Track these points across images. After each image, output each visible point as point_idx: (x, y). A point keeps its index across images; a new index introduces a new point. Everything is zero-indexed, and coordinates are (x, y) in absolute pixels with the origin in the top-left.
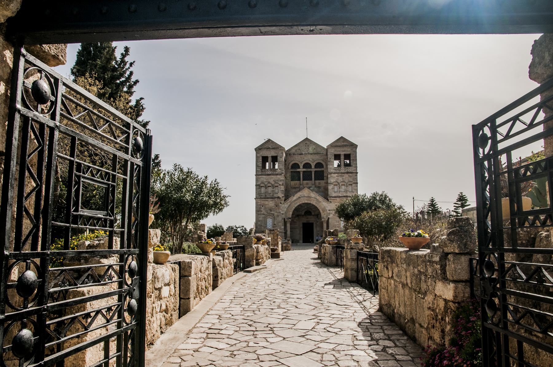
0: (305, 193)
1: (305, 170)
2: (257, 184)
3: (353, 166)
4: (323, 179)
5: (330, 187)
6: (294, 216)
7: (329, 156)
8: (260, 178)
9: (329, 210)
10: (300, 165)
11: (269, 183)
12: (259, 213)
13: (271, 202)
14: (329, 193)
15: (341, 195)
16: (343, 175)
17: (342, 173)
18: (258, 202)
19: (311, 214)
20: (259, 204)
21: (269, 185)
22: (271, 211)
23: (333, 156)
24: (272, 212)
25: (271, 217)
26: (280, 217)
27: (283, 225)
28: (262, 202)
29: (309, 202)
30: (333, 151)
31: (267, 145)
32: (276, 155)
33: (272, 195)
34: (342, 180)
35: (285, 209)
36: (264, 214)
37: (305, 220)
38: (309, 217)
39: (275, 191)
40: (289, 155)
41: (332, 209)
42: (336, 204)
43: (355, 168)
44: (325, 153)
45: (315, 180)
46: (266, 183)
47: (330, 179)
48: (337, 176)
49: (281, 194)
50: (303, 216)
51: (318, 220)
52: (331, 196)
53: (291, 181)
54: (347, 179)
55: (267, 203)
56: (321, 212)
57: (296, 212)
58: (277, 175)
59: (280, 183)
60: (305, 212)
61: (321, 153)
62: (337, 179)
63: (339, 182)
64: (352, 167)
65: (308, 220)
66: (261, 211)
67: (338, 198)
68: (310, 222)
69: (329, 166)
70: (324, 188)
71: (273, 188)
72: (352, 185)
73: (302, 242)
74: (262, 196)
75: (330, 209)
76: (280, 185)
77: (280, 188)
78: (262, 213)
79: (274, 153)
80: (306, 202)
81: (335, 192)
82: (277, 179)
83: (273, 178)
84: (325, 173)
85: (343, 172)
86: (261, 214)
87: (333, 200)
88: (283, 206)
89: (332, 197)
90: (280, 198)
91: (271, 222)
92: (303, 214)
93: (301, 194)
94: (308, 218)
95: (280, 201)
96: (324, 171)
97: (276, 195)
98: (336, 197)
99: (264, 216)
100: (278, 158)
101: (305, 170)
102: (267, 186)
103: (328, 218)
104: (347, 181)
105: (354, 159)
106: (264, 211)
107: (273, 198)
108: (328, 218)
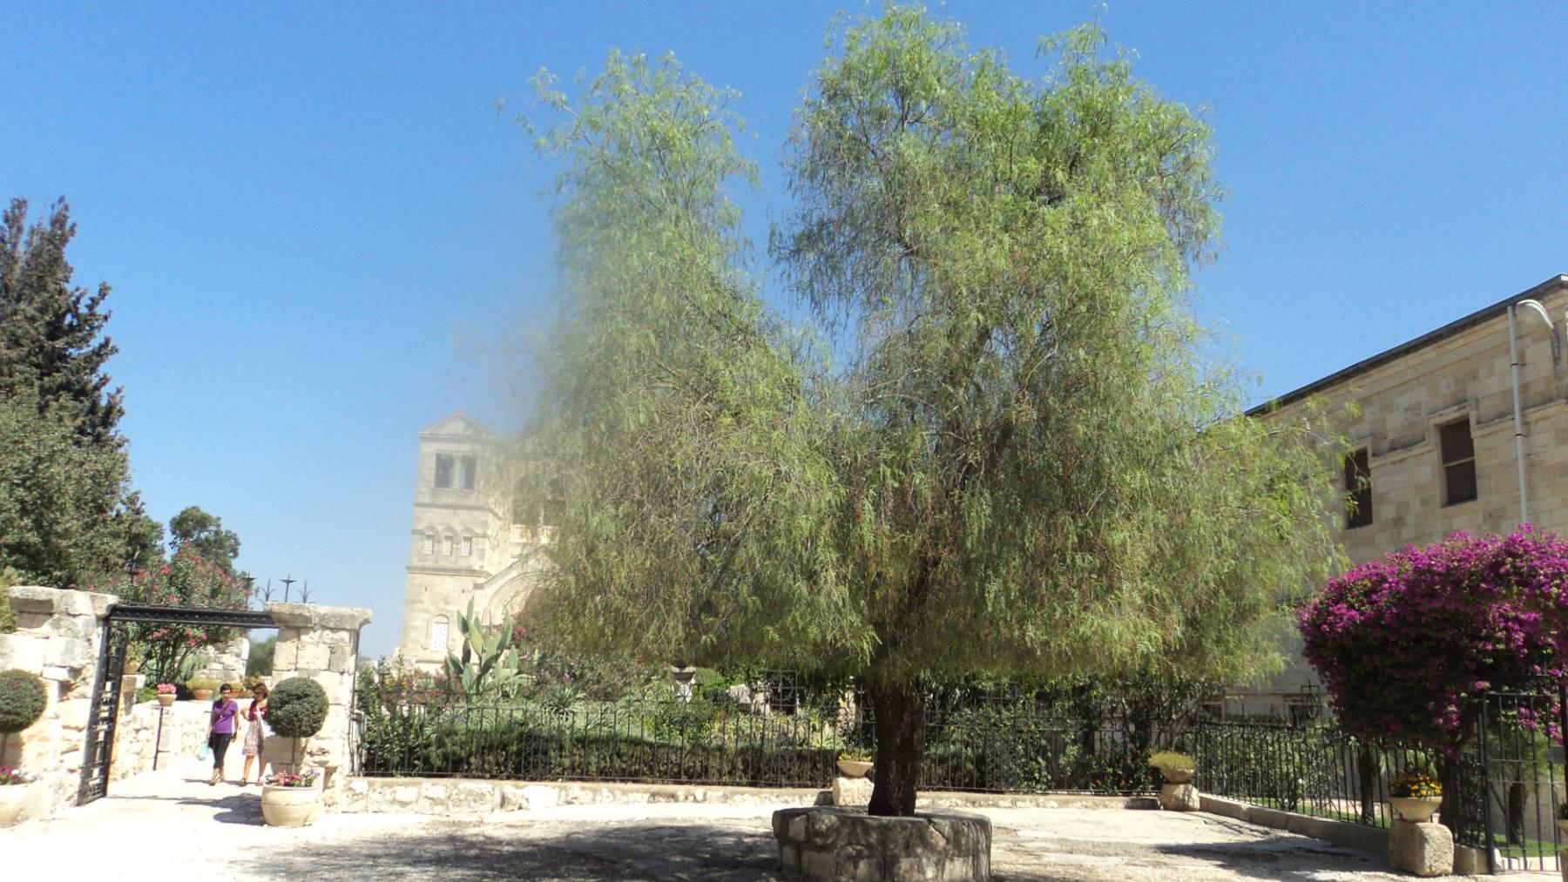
12: (415, 606)
21: (450, 534)
22: (447, 603)
25: (445, 620)
39: (460, 550)
46: (440, 528)
55: (436, 580)
66: (422, 602)
74: (426, 560)
76: (477, 535)
78: (425, 606)
97: (463, 564)
102: (443, 536)
107: (455, 572)
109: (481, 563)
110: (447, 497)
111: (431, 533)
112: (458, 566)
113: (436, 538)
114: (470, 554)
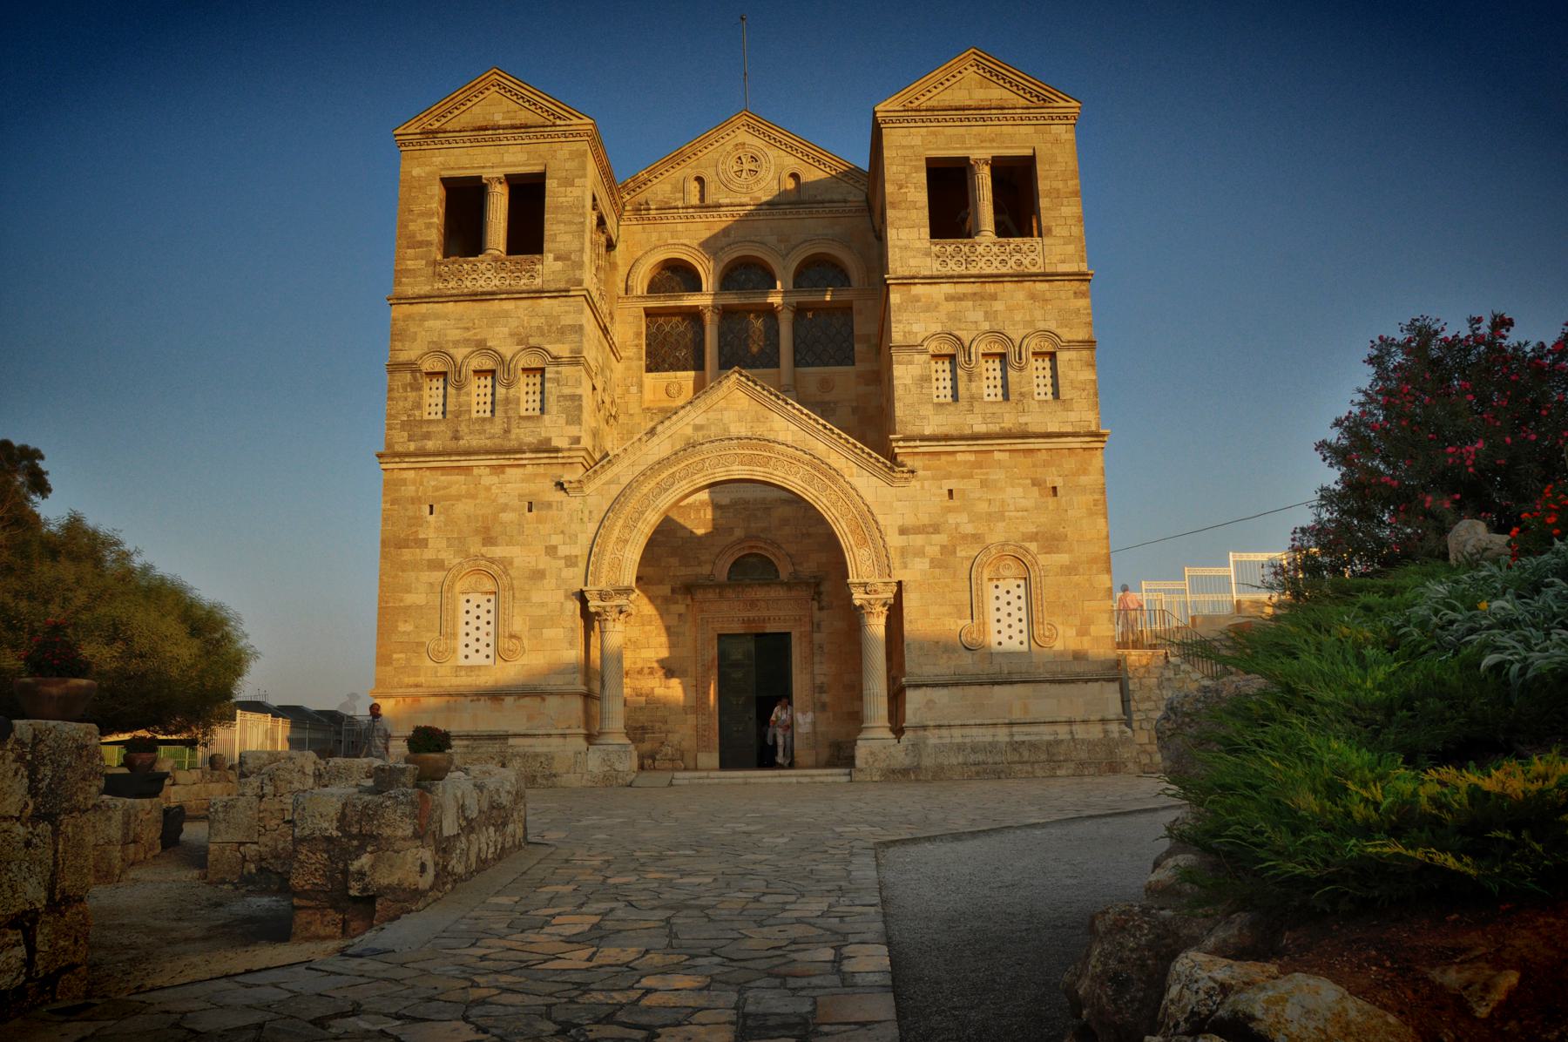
0: (728, 416)
1: (732, 299)
2: (403, 357)
3: (1057, 231)
4: (848, 359)
5: (904, 373)
6: (666, 590)
7: (893, 170)
8: (424, 318)
9: (903, 531)
10: (700, 269)
11: (482, 347)
12: (407, 554)
13: (495, 479)
14: (900, 411)
15: (980, 428)
16: (991, 288)
17: (984, 278)
18: (404, 482)
19: (778, 577)
20: (410, 491)
21: (488, 364)
22: (489, 541)
23: (917, 170)
24: (498, 552)
25: (489, 585)
26: (550, 582)
27: (571, 644)
28: (433, 481)
29: (759, 473)
30: (917, 141)
31: (476, 110)
32: (537, 169)
33: (497, 428)
34: (986, 326)
35: (592, 528)
36: (436, 565)
37: (732, 615)
38: (760, 593)
40: (637, 210)
41: (925, 520)
42: (948, 484)
43: (1071, 249)
44: (856, 196)
45: (797, 364)
46: (460, 353)
47: (905, 316)
48: (950, 298)
49: (562, 421)
50: (721, 586)
51: (818, 615)
52: (912, 430)
53: (649, 370)
54: (1018, 317)
56: (847, 540)
57: (674, 561)
58: (538, 294)
59: (555, 349)
60: (735, 564)
61: (835, 197)
62: (952, 317)
63: (966, 337)
64: (1047, 240)
65: (752, 614)
66: (423, 543)
67: (961, 446)
68: (771, 628)
69: (891, 234)
70: (855, 410)
71: (509, 386)
72: (1052, 356)
73: (713, 759)
74: (427, 436)
75: (910, 521)
76: (556, 360)
77: (558, 381)
78: (429, 554)
79: (522, 157)
80: (739, 471)
81: (941, 405)
82: (535, 323)
83: (506, 315)
84: (857, 319)
85: (988, 271)
86: (415, 566)
87: (926, 460)
88: (573, 503)
89: (923, 438)
90: (557, 450)
91: (485, 617)
92: (722, 574)
93: (698, 421)
94: (753, 604)
95: (557, 471)
96: (855, 308)
97: (525, 434)
98: (947, 438)
99: (438, 576)
100: (551, 184)
101: (732, 299)
103: (900, 583)
104: (1016, 334)
105: (1058, 190)
106: (444, 544)
107: (506, 452)
108: (900, 583)
109: (574, 431)
110: (483, 273)
111: (439, 368)
112: (514, 444)
113: (451, 378)
114: (542, 410)
